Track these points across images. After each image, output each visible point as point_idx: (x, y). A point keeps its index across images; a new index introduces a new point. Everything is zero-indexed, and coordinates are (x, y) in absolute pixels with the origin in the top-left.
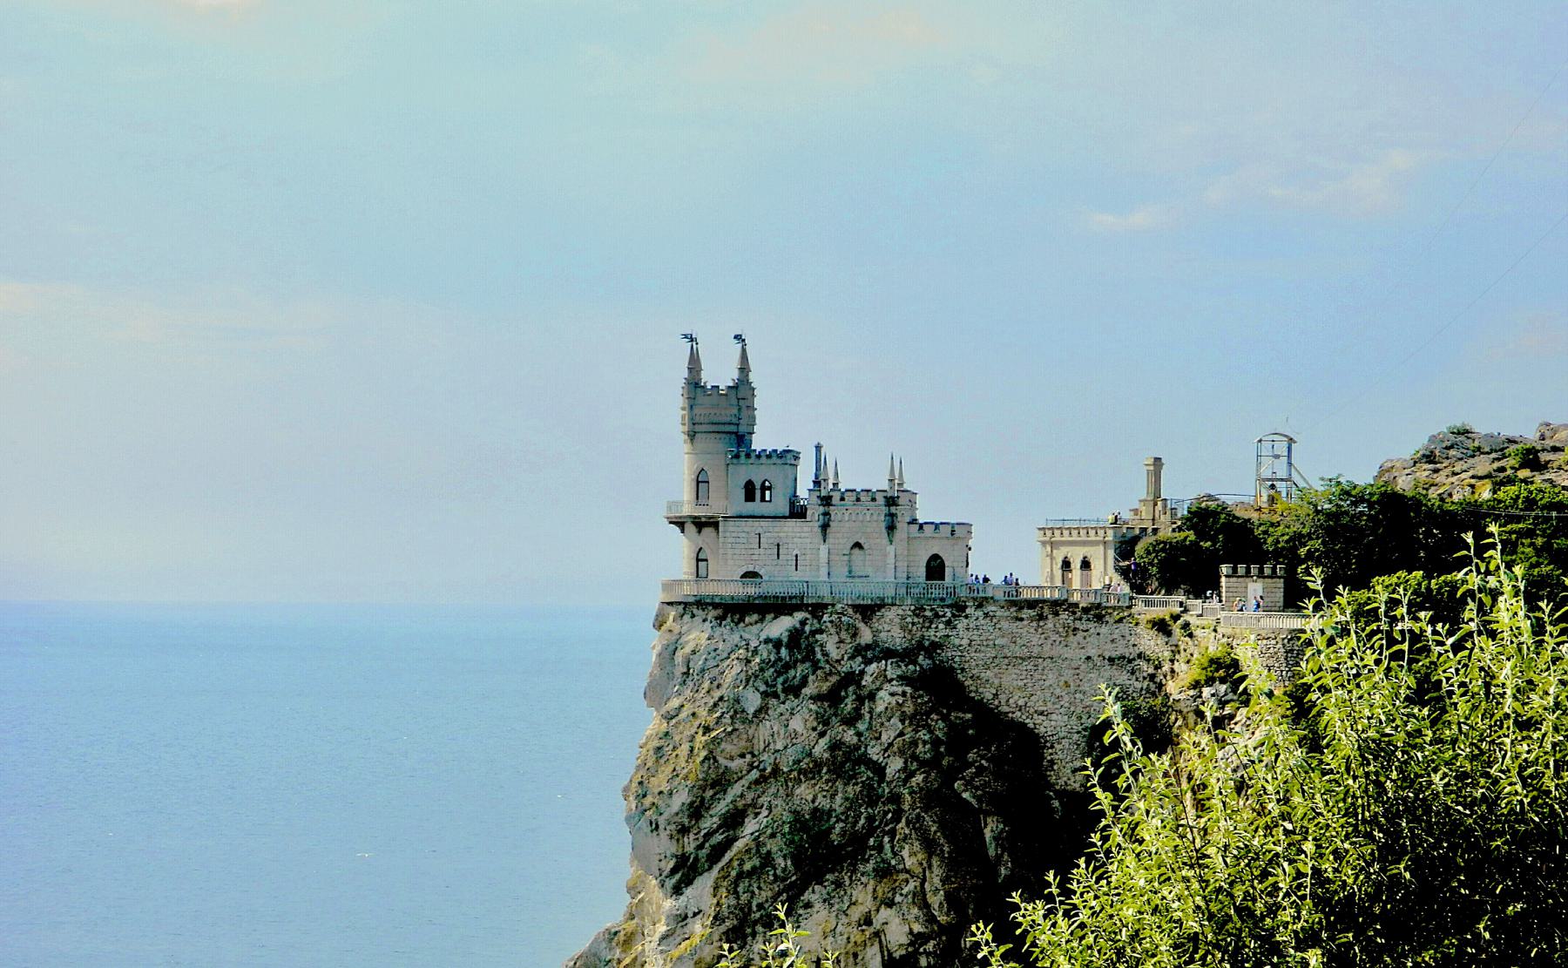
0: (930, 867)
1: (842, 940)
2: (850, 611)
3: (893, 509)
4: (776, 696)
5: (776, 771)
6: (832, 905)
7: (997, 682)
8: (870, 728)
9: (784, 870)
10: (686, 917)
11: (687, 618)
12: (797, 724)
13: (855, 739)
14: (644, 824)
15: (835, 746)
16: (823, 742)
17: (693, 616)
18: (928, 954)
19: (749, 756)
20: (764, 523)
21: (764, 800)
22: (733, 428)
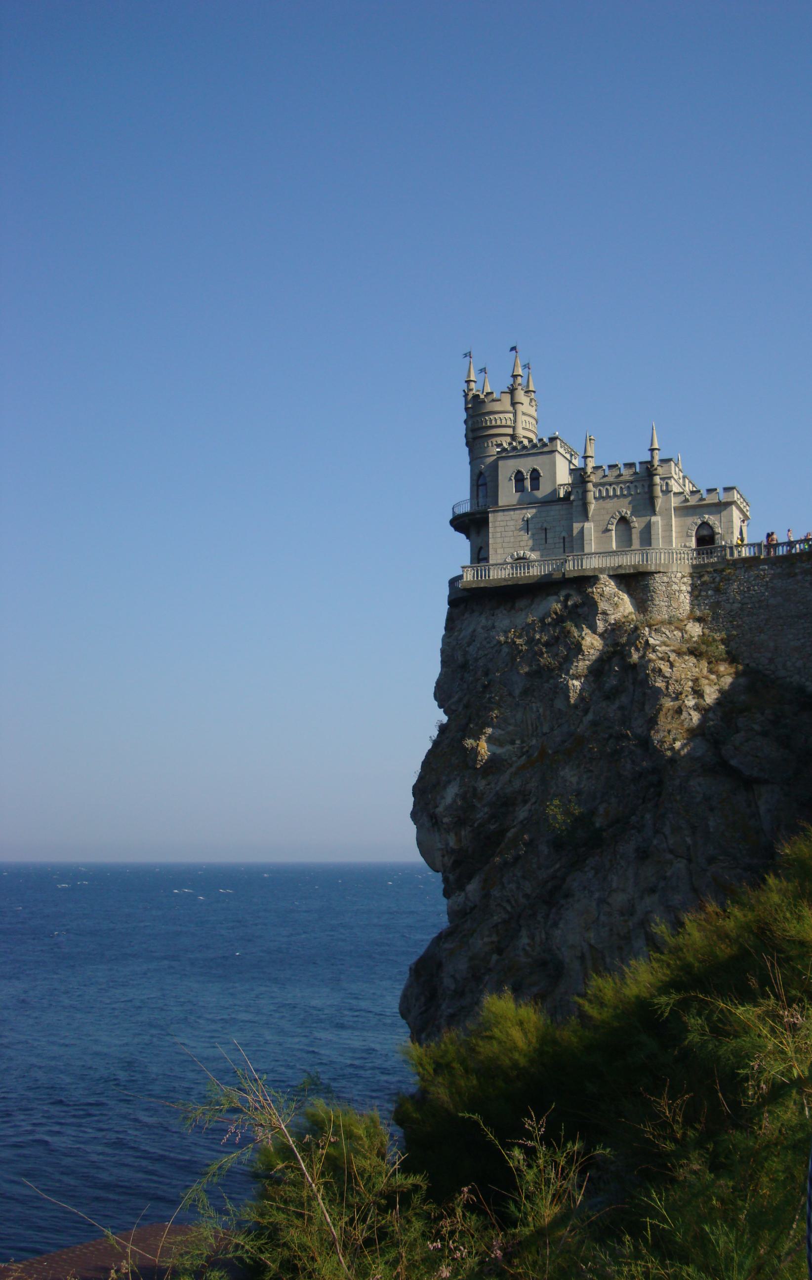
11: (467, 615)
17: (473, 611)
19: (518, 742)
20: (530, 511)
22: (510, 431)
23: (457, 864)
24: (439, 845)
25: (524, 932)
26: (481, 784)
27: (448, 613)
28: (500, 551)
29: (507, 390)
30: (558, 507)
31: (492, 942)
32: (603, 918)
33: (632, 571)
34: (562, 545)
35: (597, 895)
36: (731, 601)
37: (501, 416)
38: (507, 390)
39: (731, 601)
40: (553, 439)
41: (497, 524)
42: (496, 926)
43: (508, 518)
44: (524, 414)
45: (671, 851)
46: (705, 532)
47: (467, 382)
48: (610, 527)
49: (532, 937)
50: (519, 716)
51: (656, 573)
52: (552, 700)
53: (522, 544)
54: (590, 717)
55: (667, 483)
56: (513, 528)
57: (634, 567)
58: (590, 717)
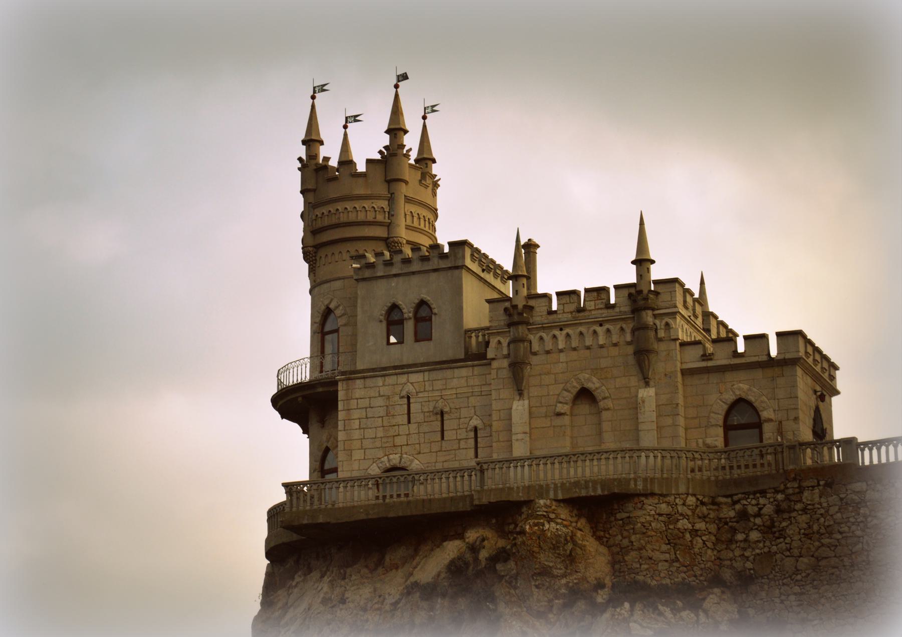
2: (564, 513)
3: (648, 317)
20: (414, 378)
22: (380, 232)
27: (268, 574)
28: (358, 455)
29: (378, 157)
30: (464, 372)
33: (599, 492)
34: (472, 442)
36: (796, 552)
37: (367, 204)
38: (378, 157)
39: (796, 552)
41: (353, 403)
43: (373, 393)
44: (408, 200)
47: (304, 142)
48: (561, 408)
51: (646, 495)
53: (399, 441)
55: (667, 324)
56: (382, 412)
57: (604, 483)
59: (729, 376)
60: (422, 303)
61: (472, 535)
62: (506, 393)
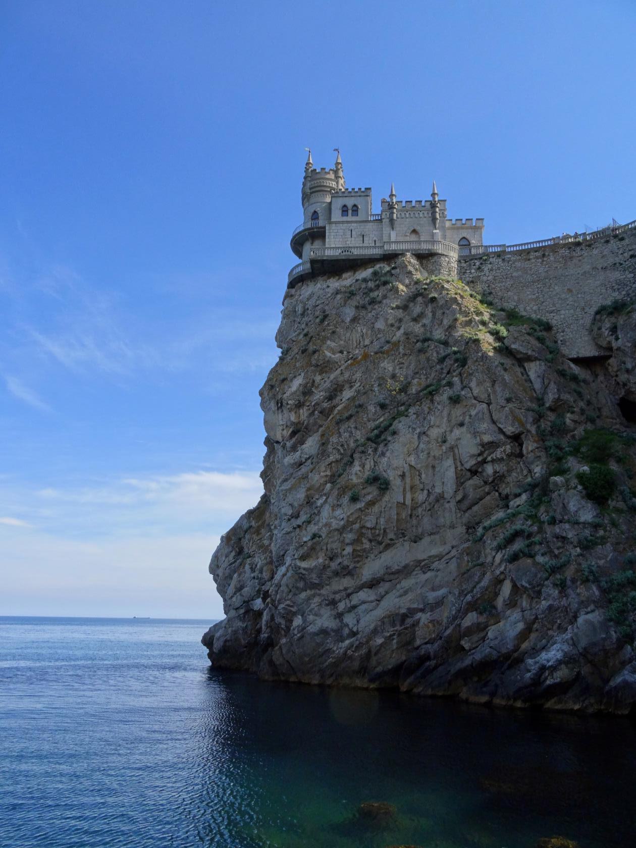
0: (495, 392)
1: (423, 456)
4: (364, 307)
5: (366, 356)
6: (414, 429)
7: (516, 298)
8: (432, 322)
9: (375, 413)
10: (301, 464)
12: (380, 325)
13: (422, 330)
14: (273, 405)
15: (406, 334)
16: (399, 333)
18: (493, 461)
21: (358, 375)
23: (294, 433)
24: (281, 423)
25: (357, 463)
26: (318, 378)
31: (326, 476)
32: (422, 446)
35: (418, 430)
40: (368, 189)
42: (330, 464)
45: (475, 398)
46: (462, 243)
49: (363, 466)
50: (348, 335)
52: (373, 323)
54: (402, 331)
58: (402, 331)
59: (461, 231)
60: (355, 206)
61: (377, 267)
62: (388, 229)
